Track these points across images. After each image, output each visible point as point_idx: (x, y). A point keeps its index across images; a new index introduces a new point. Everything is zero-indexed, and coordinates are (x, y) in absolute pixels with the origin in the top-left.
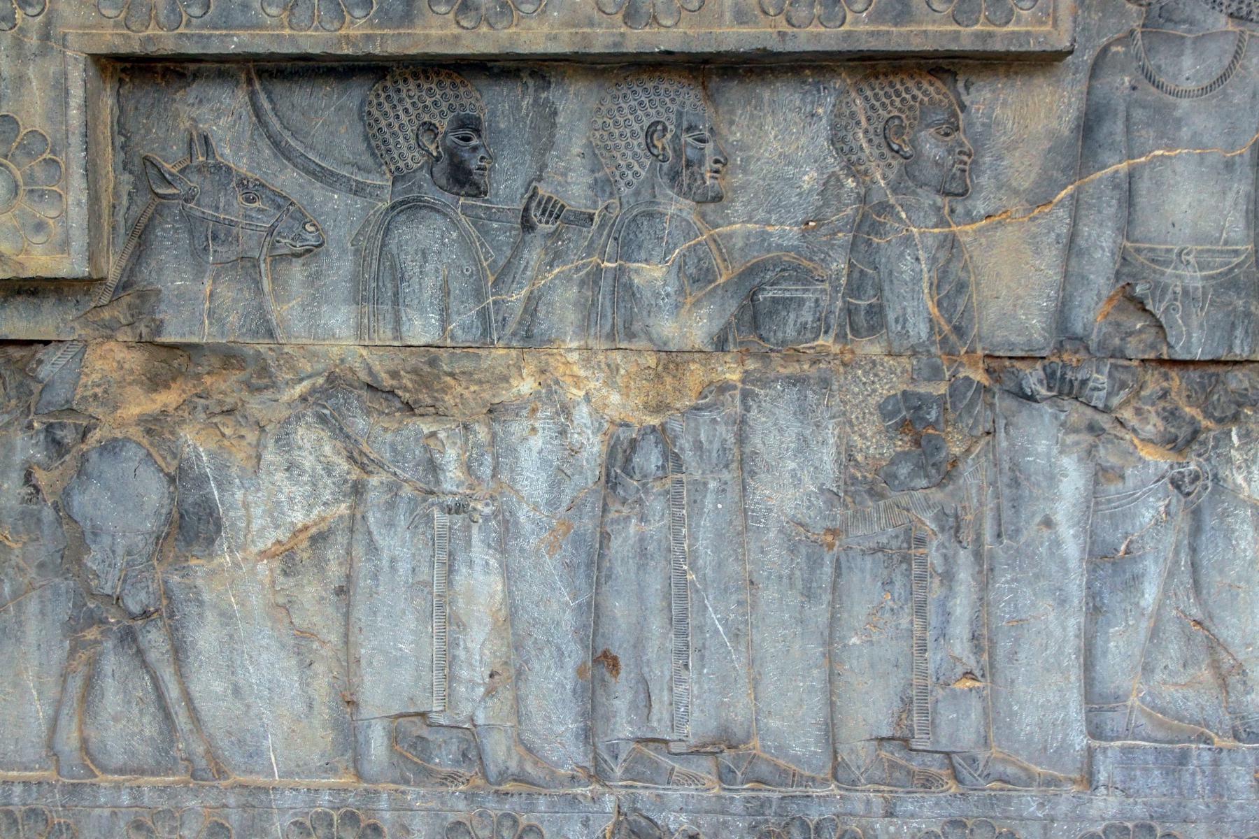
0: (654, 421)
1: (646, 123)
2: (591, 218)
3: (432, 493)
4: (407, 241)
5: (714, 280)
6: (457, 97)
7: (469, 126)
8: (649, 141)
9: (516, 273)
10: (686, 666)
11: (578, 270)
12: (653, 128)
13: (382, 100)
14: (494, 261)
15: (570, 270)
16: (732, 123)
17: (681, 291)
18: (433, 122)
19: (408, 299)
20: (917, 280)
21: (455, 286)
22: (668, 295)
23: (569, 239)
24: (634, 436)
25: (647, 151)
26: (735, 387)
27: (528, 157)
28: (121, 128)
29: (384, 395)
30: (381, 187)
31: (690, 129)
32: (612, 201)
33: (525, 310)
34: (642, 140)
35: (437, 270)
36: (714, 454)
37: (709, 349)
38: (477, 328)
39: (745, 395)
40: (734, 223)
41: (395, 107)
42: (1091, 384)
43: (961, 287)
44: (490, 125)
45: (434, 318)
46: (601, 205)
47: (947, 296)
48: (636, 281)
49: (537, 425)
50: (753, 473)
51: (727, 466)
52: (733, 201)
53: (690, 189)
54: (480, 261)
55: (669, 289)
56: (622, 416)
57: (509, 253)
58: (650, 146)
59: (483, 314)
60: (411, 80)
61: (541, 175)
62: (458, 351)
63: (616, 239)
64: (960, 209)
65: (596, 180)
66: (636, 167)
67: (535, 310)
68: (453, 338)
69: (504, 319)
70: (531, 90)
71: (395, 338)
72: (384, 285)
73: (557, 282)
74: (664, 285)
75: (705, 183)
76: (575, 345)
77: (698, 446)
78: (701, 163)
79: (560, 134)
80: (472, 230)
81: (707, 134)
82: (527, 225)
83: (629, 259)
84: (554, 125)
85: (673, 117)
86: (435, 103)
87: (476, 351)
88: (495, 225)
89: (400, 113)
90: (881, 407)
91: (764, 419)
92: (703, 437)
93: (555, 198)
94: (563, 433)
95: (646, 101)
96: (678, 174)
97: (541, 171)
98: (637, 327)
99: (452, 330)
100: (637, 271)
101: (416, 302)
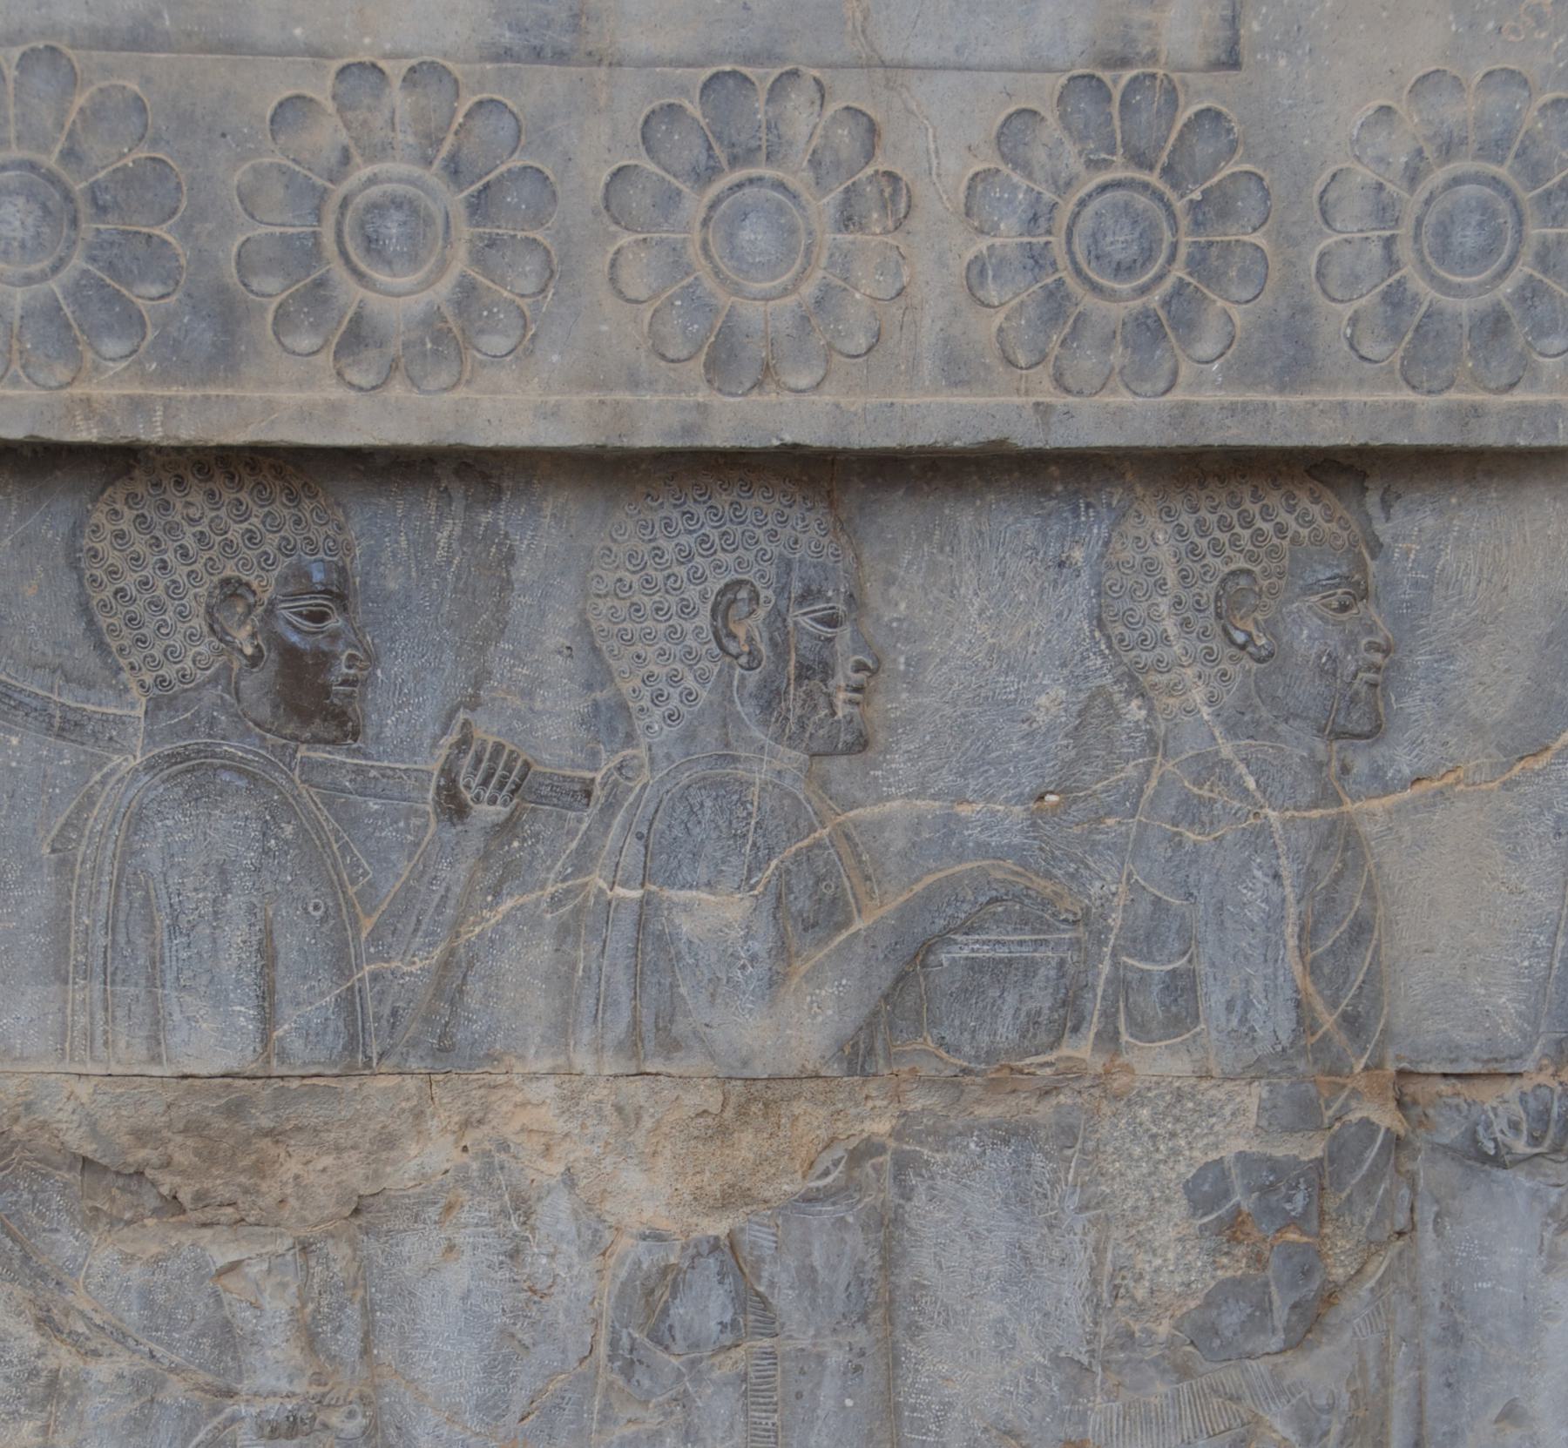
0: (718, 1227)
4: (185, 844)
5: (847, 923)
6: (298, 522)
8: (720, 623)
9: (423, 912)
11: (556, 902)
12: (730, 596)
13: (125, 525)
14: (370, 884)
15: (537, 903)
16: (890, 580)
17: (783, 951)
18: (245, 578)
19: (188, 973)
21: (287, 945)
22: (753, 959)
23: (536, 835)
24: (673, 1260)
25: (714, 645)
26: (881, 1149)
27: (449, 655)
29: (120, 1182)
30: (120, 721)
31: (807, 596)
32: (629, 752)
33: (439, 993)
34: (704, 619)
35: (251, 909)
36: (840, 1294)
37: (834, 1070)
38: (336, 1033)
39: (903, 1164)
40: (889, 798)
41: (157, 542)
43: (1361, 930)
44: (365, 584)
45: (245, 1016)
46: (607, 763)
47: (1331, 951)
48: (686, 926)
49: (459, 1239)
50: (914, 1330)
51: (863, 1318)
52: (887, 750)
53: (803, 727)
54: (342, 885)
55: (756, 946)
56: (646, 1216)
57: (405, 867)
59: (349, 1004)
60: (191, 479)
61: (476, 696)
62: (295, 1084)
63: (640, 836)
65: (596, 704)
66: (690, 682)
67: (461, 992)
68: (283, 1056)
69: (394, 1013)
70: (457, 507)
71: (155, 1059)
72: (129, 942)
73: (508, 928)
74: (746, 938)
75: (834, 714)
76: (545, 1064)
77: (807, 1277)
78: (827, 670)
79: (520, 603)
80: (323, 815)
81: (841, 608)
82: (453, 806)
83: (670, 882)
84: (507, 584)
85: (771, 571)
86: (251, 536)
87: (333, 1083)
88: (374, 805)
89: (169, 556)
90: (1190, 1188)
91: (940, 1215)
92: (817, 1259)
93: (509, 747)
94: (514, 1254)
95: (714, 535)
96: (779, 694)
97: (477, 685)
98: (681, 1027)
99: (281, 1039)
100: (687, 908)
101: (205, 979)
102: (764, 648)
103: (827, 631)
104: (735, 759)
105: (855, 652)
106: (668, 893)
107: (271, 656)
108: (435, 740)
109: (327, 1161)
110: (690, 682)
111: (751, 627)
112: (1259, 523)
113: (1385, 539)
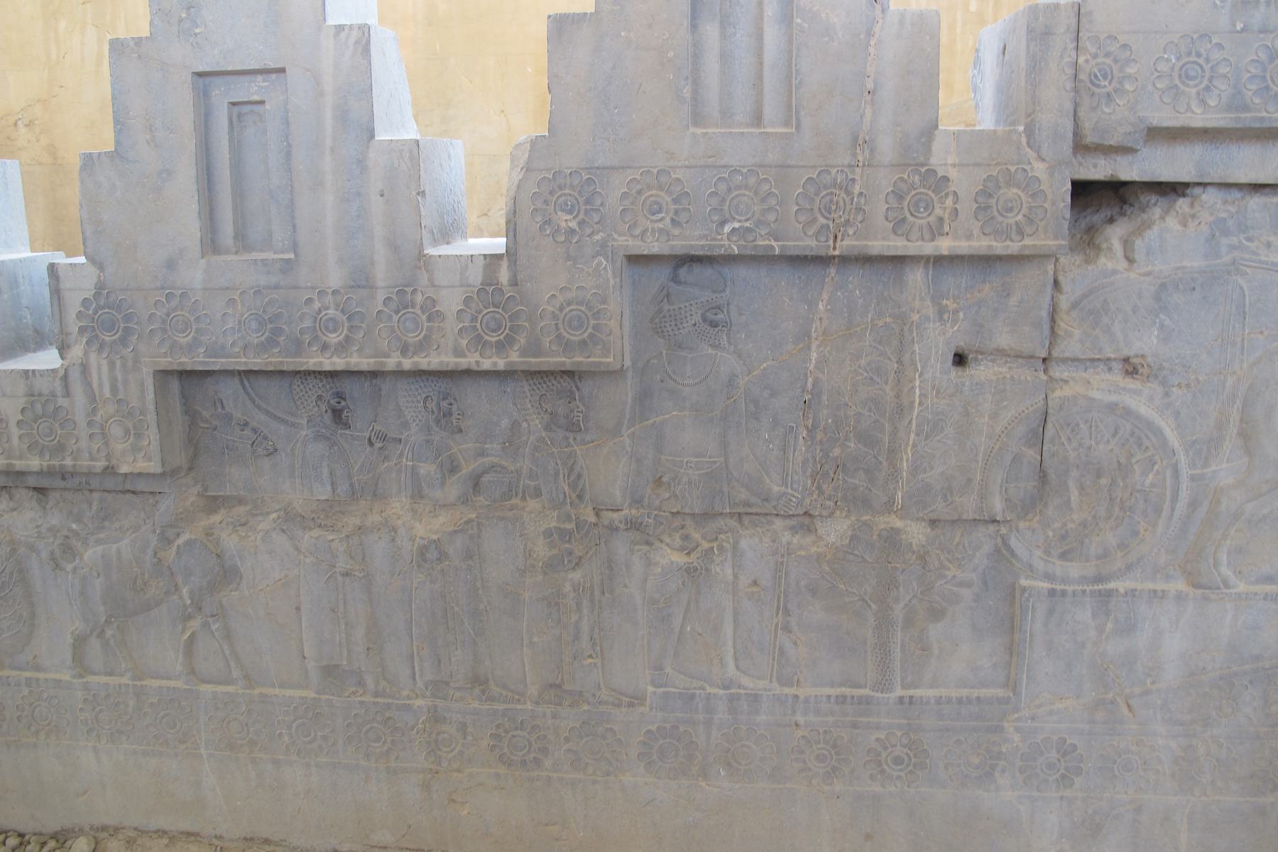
1: (424, 396)
2: (400, 440)
3: (335, 567)
7: (340, 396)
10: (457, 649)
13: (299, 383)
17: (444, 477)
20: (557, 474)
28: (183, 395)
34: (422, 404)
35: (328, 465)
39: (479, 524)
40: (469, 443)
42: (644, 523)
43: (579, 476)
45: (329, 488)
55: (438, 476)
58: (425, 407)
59: (352, 485)
64: (579, 438)
69: (362, 487)
84: (380, 395)
85: (436, 393)
86: (323, 386)
88: (356, 442)
94: (393, 540)
97: (376, 417)
102: (435, 410)
103: (450, 407)
104: (431, 434)
105: (458, 410)
106: (418, 464)
107: (329, 411)
108: (368, 429)
109: (353, 518)
110: (420, 418)
111: (432, 405)
112: (548, 383)
113: (580, 387)
